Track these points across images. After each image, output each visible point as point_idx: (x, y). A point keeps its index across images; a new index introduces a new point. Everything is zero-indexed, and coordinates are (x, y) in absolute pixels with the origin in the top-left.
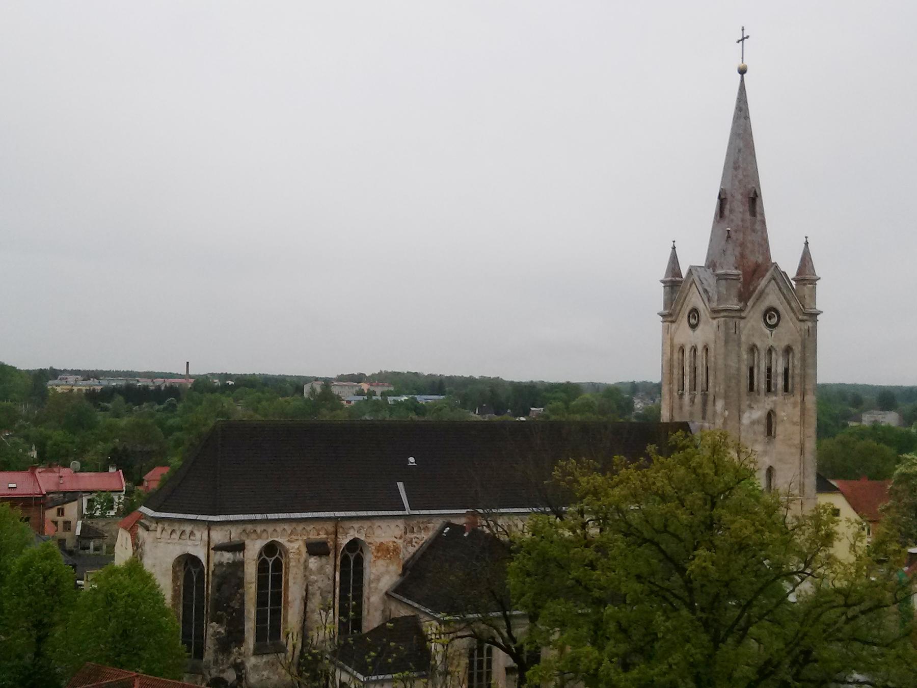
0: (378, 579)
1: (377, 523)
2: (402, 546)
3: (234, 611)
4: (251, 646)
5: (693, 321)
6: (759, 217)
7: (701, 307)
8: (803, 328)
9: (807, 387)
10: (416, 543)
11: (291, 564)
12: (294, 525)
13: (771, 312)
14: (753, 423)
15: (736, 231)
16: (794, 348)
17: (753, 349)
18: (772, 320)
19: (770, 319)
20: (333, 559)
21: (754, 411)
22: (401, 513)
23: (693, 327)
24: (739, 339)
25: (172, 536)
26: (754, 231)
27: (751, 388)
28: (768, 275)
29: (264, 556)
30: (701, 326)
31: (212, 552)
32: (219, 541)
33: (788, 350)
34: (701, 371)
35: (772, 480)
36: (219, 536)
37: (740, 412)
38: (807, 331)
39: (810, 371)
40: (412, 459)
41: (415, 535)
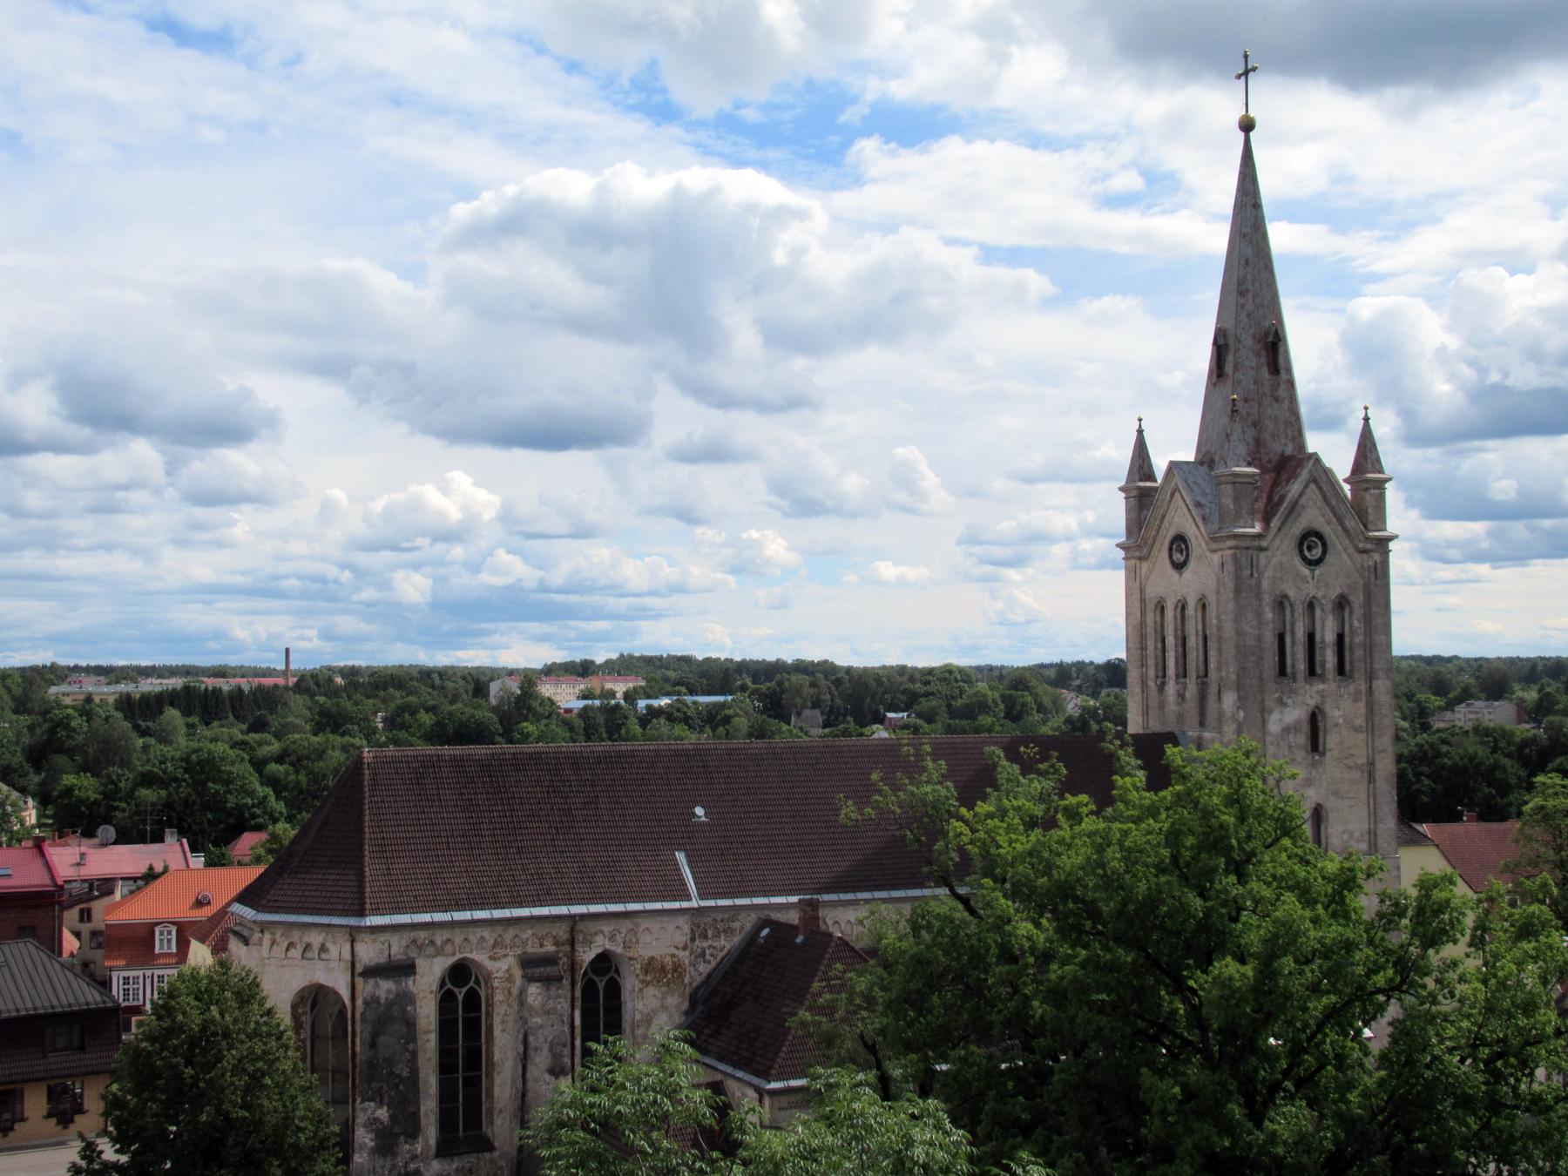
0: (648, 1021)
1: (644, 923)
2: (687, 962)
3: (402, 1081)
4: (433, 1142)
5: (1178, 557)
6: (1283, 372)
7: (1191, 531)
8: (1366, 564)
9: (1377, 666)
10: (712, 955)
11: (496, 999)
12: (499, 929)
13: (1310, 538)
14: (1287, 730)
15: (1246, 401)
16: (1351, 598)
17: (1281, 603)
18: (1314, 552)
19: (1310, 549)
20: (569, 987)
21: (1288, 709)
22: (685, 905)
23: (1179, 567)
24: (1258, 586)
25: (289, 954)
26: (1276, 400)
27: (1282, 671)
28: (1304, 474)
29: (449, 986)
30: (1192, 565)
31: (359, 981)
32: (371, 960)
33: (1341, 604)
34: (1192, 642)
35: (1323, 830)
36: (369, 952)
37: (1264, 711)
38: (1372, 570)
39: (1379, 638)
40: (699, 811)
41: (710, 942)
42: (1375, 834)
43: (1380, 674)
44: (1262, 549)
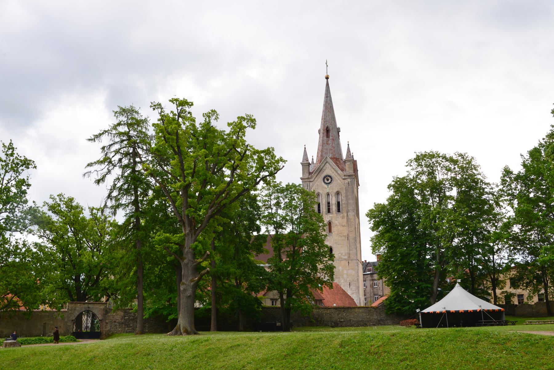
6: (331, 138)
9: (349, 209)
19: (328, 180)
33: (338, 193)
42: (350, 254)
43: (351, 211)
44: (310, 182)
